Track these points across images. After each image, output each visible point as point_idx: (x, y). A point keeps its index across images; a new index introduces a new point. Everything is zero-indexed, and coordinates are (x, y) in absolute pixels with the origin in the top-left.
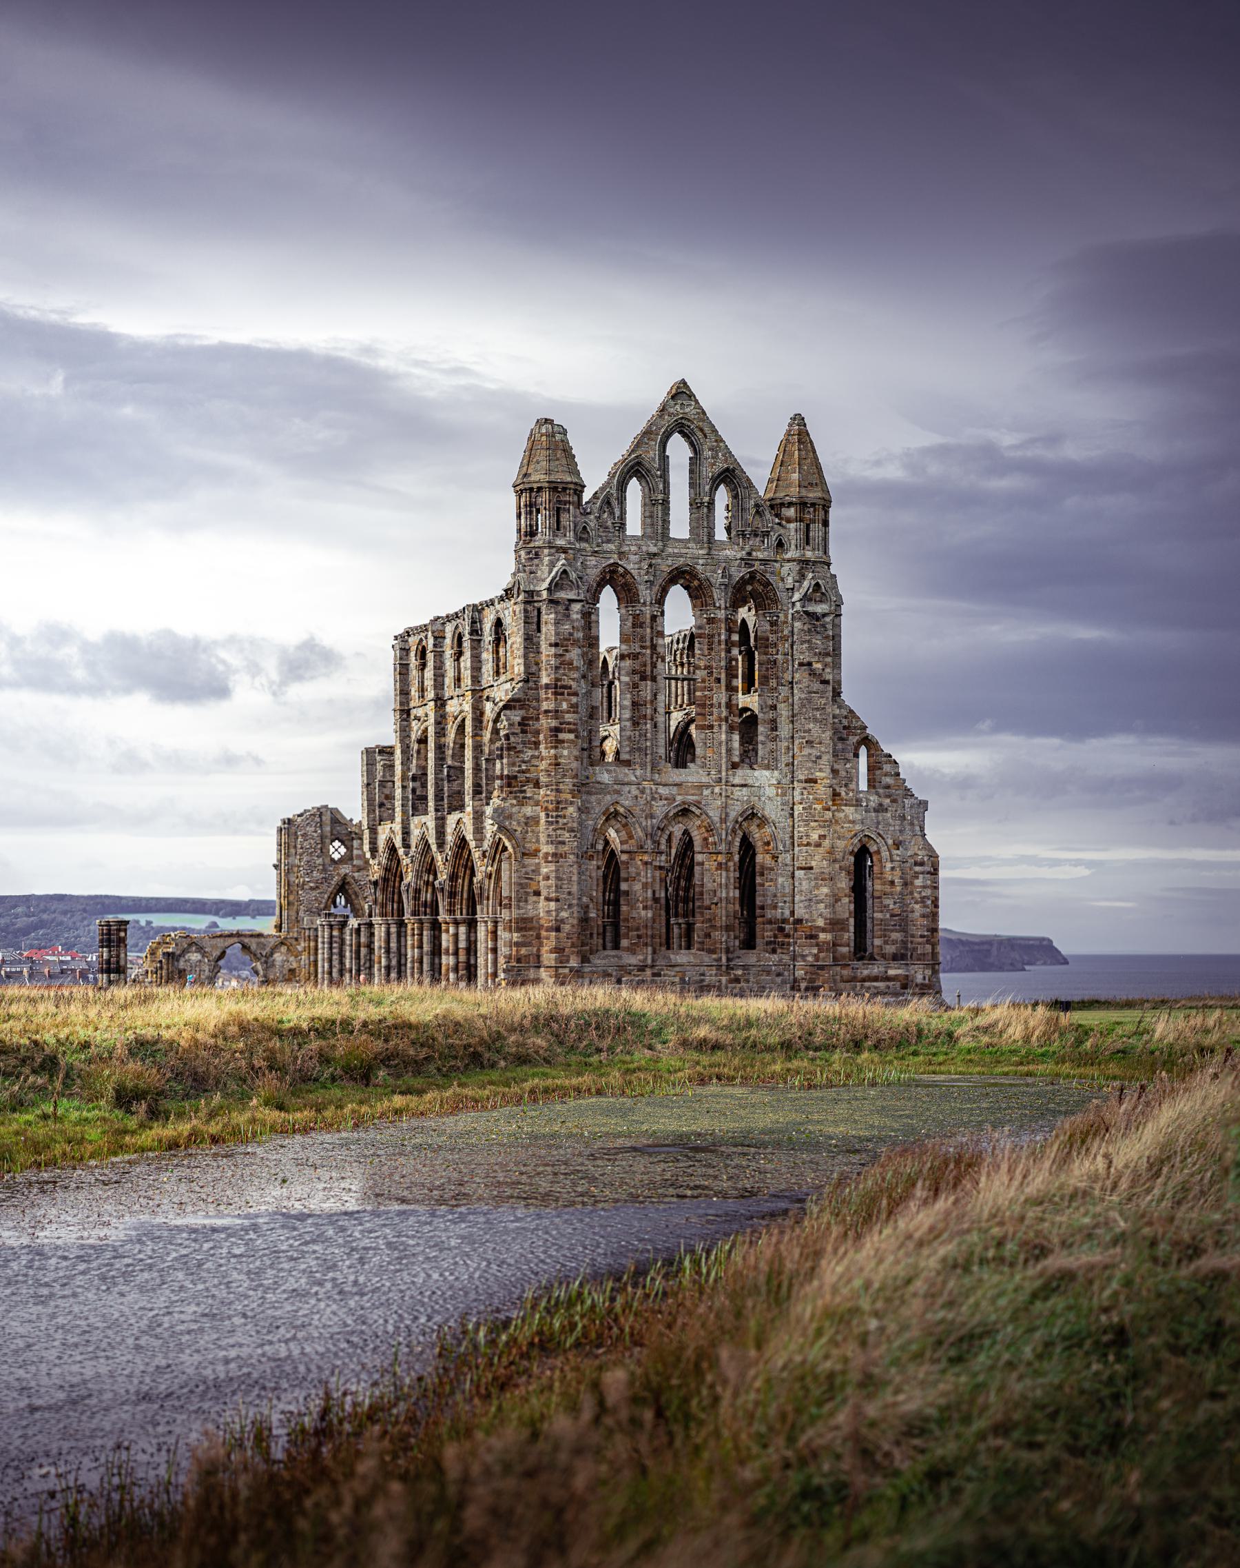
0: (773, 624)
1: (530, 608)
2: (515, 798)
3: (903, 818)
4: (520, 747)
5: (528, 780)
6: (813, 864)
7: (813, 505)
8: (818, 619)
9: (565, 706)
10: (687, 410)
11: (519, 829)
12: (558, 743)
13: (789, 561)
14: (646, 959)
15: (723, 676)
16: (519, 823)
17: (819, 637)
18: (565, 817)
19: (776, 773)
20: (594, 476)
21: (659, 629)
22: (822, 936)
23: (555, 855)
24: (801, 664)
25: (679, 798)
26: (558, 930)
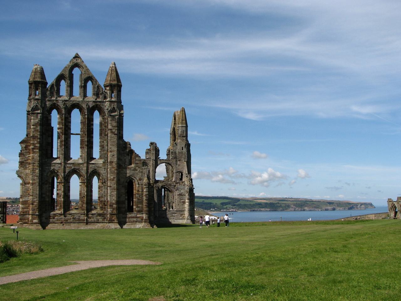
0: (103, 119)
1: (29, 116)
2: (23, 168)
3: (142, 172)
4: (25, 154)
5: (27, 163)
6: (112, 185)
7: (114, 86)
8: (114, 117)
9: (36, 142)
10: (78, 61)
11: (24, 176)
12: (34, 152)
13: (107, 101)
14: (62, 212)
15: (86, 133)
16: (24, 175)
17: (114, 122)
18: (35, 173)
19: (103, 160)
20: (50, 80)
21: (69, 121)
22: (114, 205)
23: (32, 183)
24: (109, 130)
25: (73, 167)
26: (33, 204)
